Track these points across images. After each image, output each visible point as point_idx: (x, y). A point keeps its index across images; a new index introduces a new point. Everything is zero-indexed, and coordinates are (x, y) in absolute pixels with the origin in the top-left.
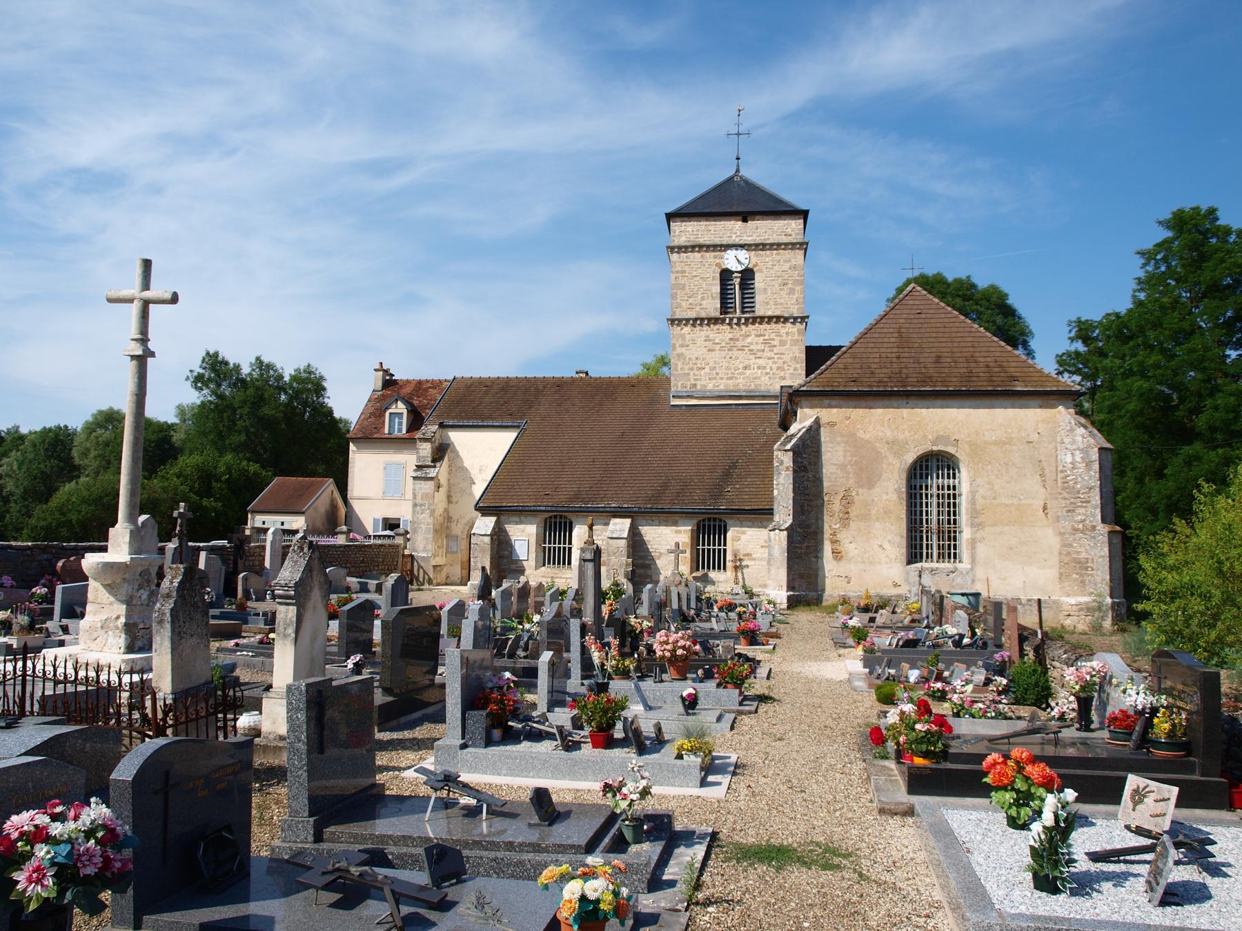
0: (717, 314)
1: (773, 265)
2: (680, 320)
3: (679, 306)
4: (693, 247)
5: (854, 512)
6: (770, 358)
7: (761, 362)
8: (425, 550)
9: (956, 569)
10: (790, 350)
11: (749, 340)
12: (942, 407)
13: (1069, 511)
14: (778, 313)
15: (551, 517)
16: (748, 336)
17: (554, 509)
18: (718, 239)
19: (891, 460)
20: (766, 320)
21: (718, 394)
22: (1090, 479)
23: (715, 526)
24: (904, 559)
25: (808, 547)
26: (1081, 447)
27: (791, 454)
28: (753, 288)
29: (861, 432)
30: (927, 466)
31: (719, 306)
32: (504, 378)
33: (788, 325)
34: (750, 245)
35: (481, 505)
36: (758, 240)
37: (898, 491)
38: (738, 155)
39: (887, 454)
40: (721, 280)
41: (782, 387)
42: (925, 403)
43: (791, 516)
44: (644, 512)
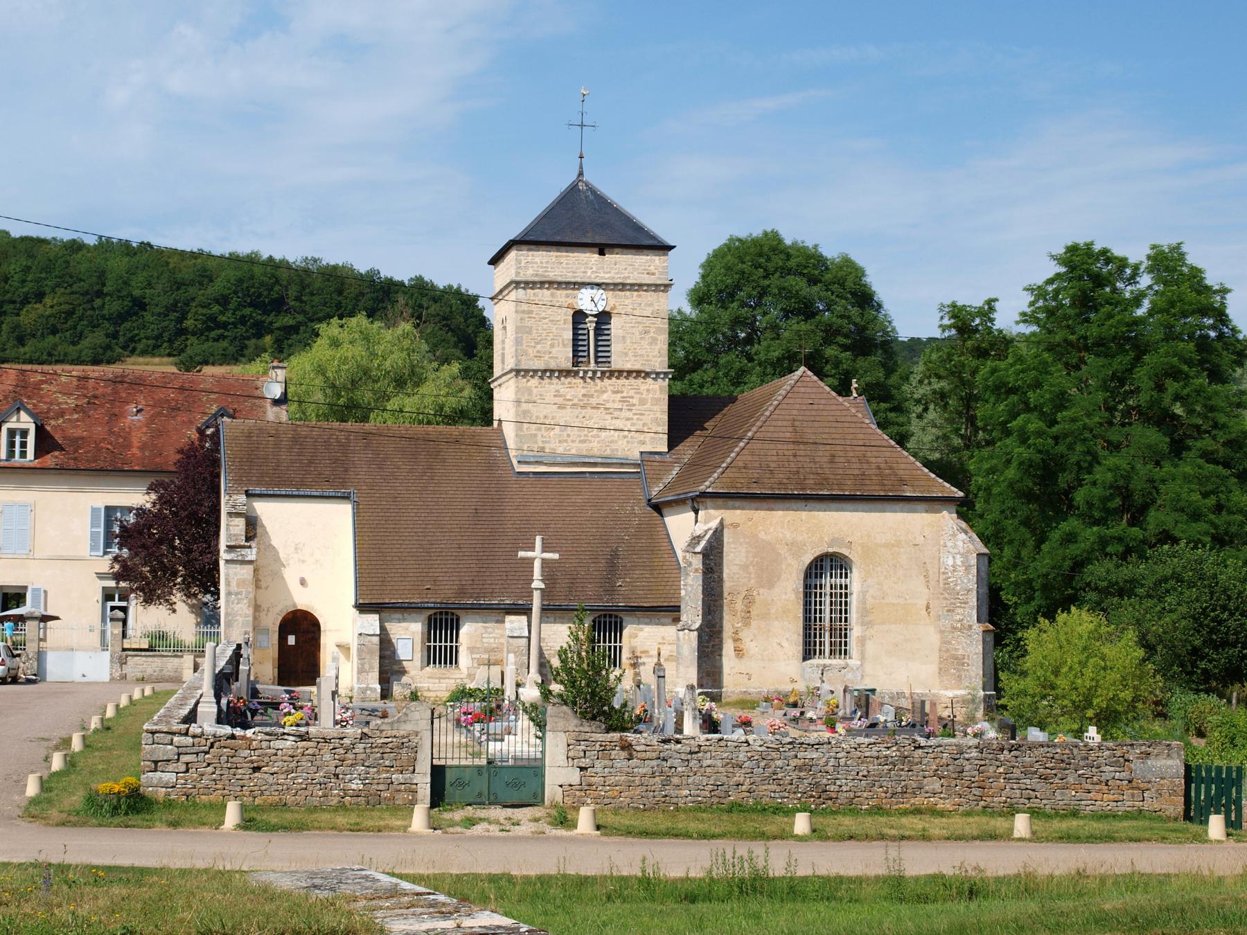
0: (568, 365)
2: (527, 371)
4: (542, 283)
6: (628, 419)
9: (847, 665)
11: (605, 396)
12: (837, 510)
13: (949, 611)
14: (637, 367)
15: (435, 614)
16: (605, 392)
17: (443, 606)
18: (570, 274)
20: (625, 374)
21: (570, 460)
23: (610, 623)
24: (800, 656)
25: (713, 646)
27: (701, 556)
28: (609, 335)
29: (763, 533)
30: (821, 566)
33: (649, 381)
34: (607, 284)
35: (361, 601)
38: (581, 154)
40: (573, 323)
41: (641, 453)
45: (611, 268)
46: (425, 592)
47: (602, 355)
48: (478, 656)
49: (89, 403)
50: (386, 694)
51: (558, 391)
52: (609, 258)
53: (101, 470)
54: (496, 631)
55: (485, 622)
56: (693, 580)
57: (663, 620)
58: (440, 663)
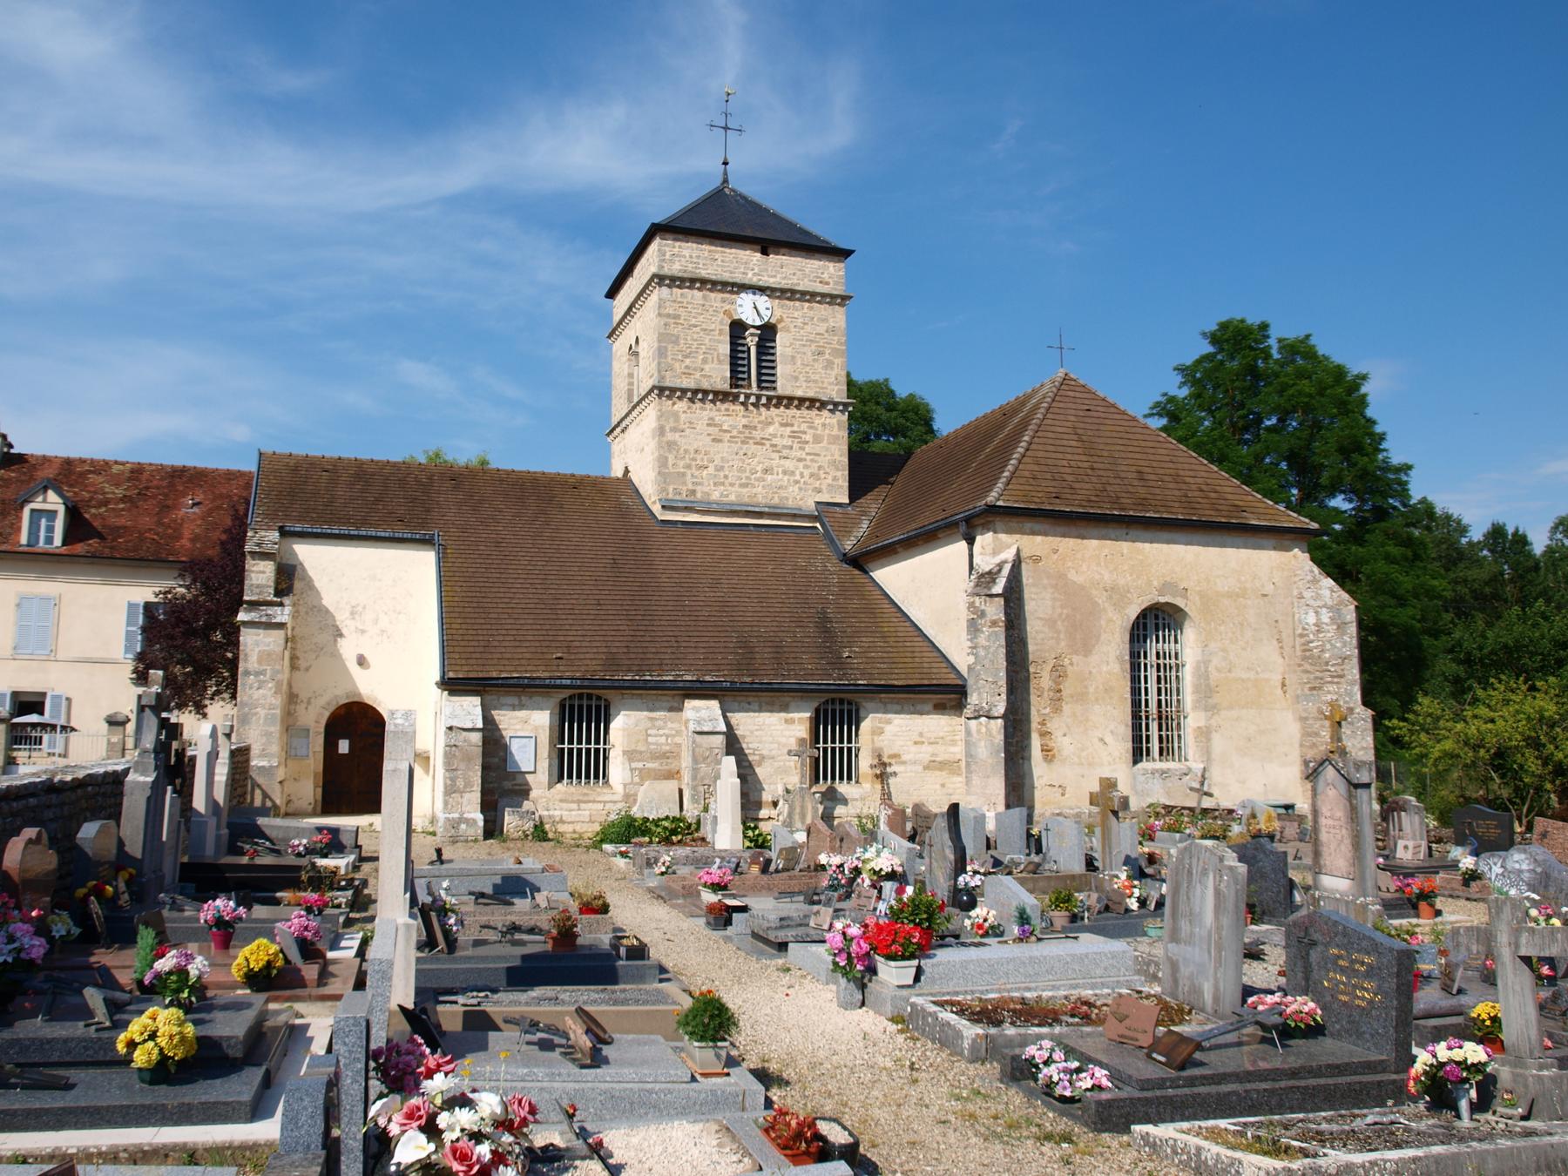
0: (725, 386)
2: (673, 390)
4: (693, 281)
5: (1068, 688)
6: (800, 460)
7: (788, 464)
8: (263, 755)
9: (1190, 769)
10: (827, 450)
11: (771, 429)
12: (1168, 542)
13: (1314, 688)
14: (810, 394)
19: (1110, 615)
20: (796, 402)
22: (1345, 646)
23: (842, 712)
24: (1129, 756)
26: (1330, 603)
27: (1001, 601)
28: (773, 354)
29: (1073, 572)
30: (1145, 625)
31: (728, 374)
32: (349, 460)
33: (825, 413)
34: (773, 290)
35: (451, 675)
36: (785, 284)
37: (1120, 659)
39: (1106, 605)
41: (818, 503)
42: (1148, 534)
43: (1004, 696)
45: (778, 272)
46: (556, 662)
47: (766, 376)
48: (640, 765)
49: (139, 494)
50: (493, 829)
53: (141, 559)
54: (670, 725)
55: (651, 710)
57: (919, 707)
58: (579, 777)
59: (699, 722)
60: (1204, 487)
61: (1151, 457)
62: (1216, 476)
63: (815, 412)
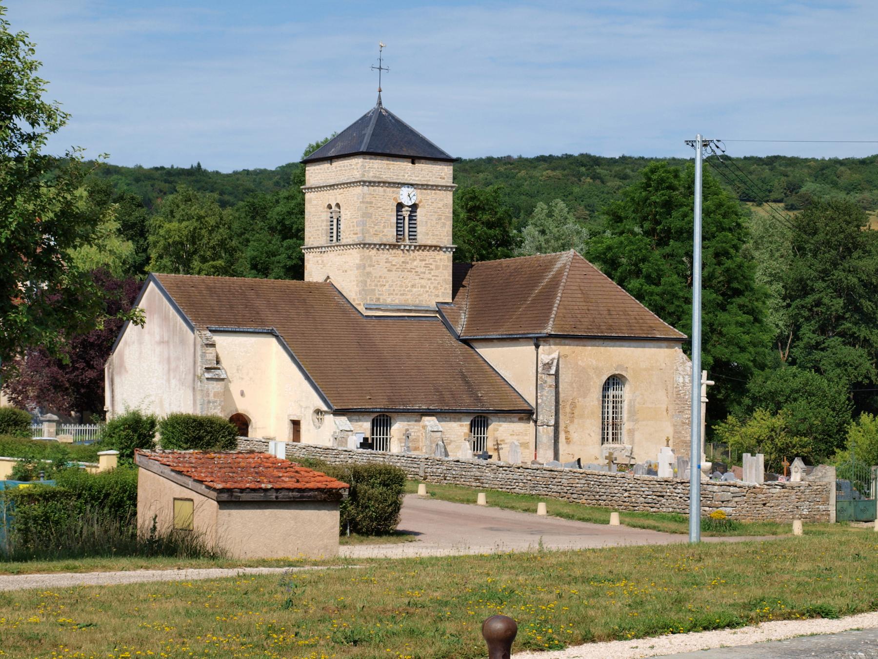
0: (393, 241)
1: (432, 203)
2: (370, 244)
3: (368, 232)
4: (379, 182)
5: (576, 412)
6: (429, 279)
7: (423, 282)
11: (415, 263)
14: (434, 243)
24: (600, 442)
27: (554, 377)
30: (609, 383)
33: (441, 252)
34: (417, 185)
41: (437, 303)
43: (554, 417)
44: (444, 412)
47: (413, 236)
51: (387, 259)
52: (419, 166)
56: (548, 392)
57: (513, 419)
59: (431, 427)
60: (637, 317)
61: (614, 301)
62: (642, 310)
63: (436, 252)
